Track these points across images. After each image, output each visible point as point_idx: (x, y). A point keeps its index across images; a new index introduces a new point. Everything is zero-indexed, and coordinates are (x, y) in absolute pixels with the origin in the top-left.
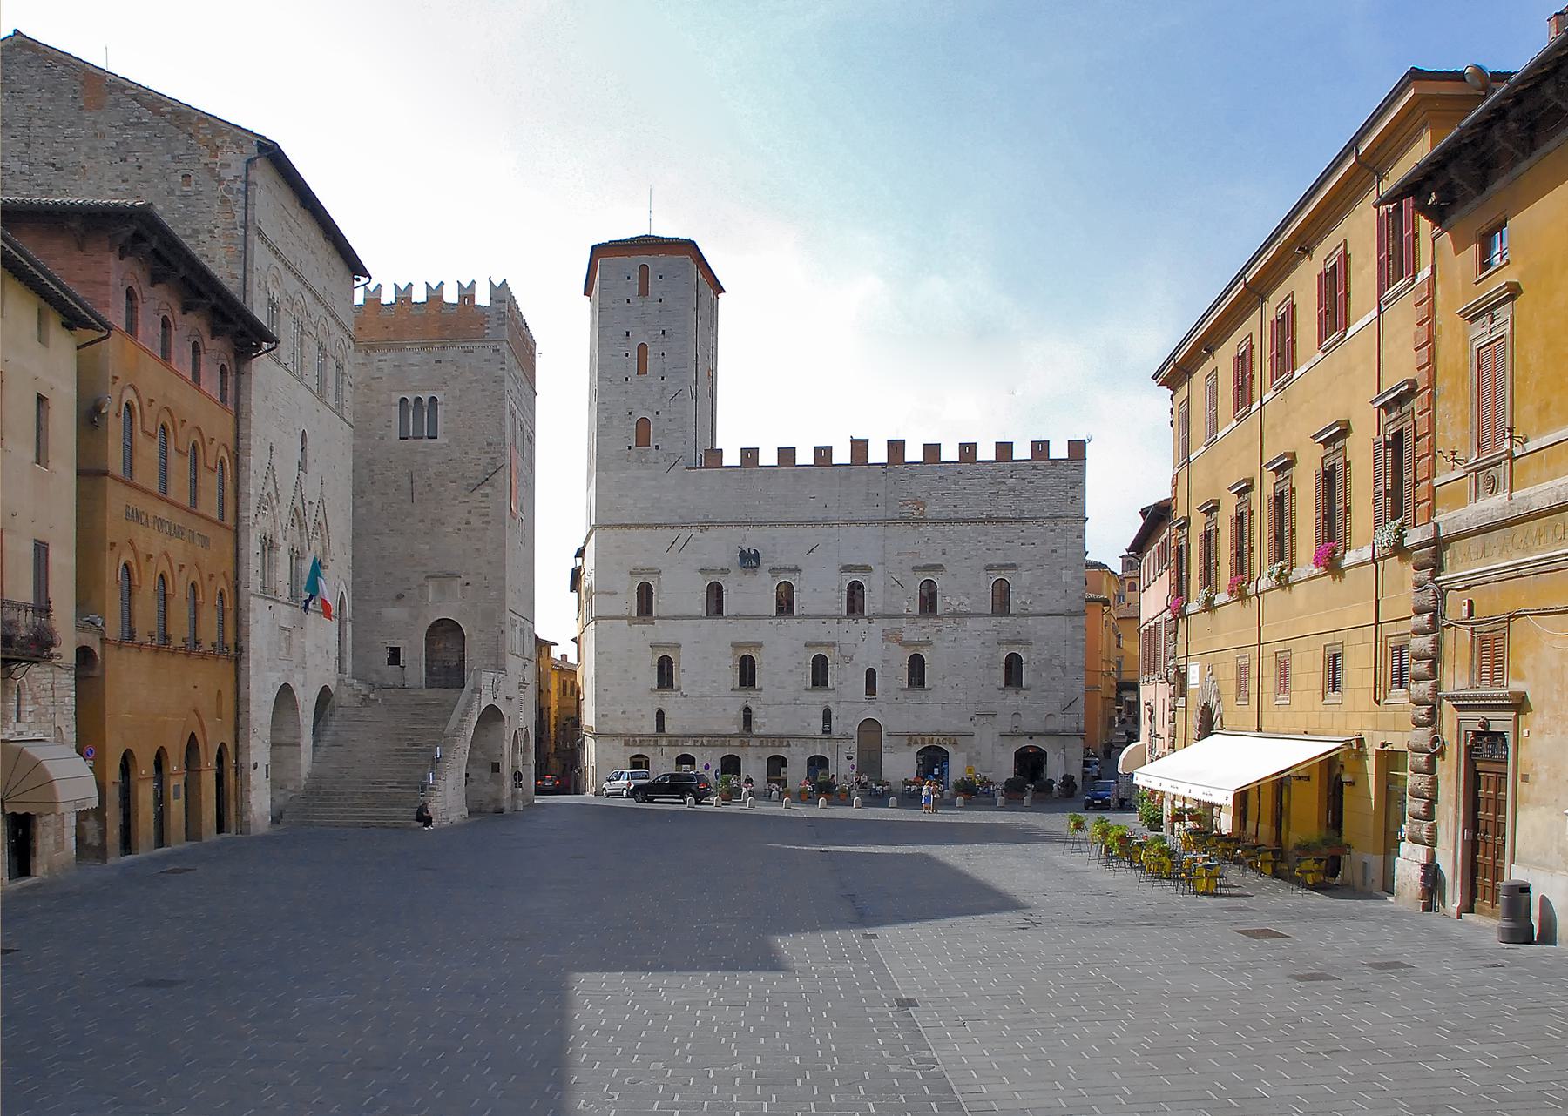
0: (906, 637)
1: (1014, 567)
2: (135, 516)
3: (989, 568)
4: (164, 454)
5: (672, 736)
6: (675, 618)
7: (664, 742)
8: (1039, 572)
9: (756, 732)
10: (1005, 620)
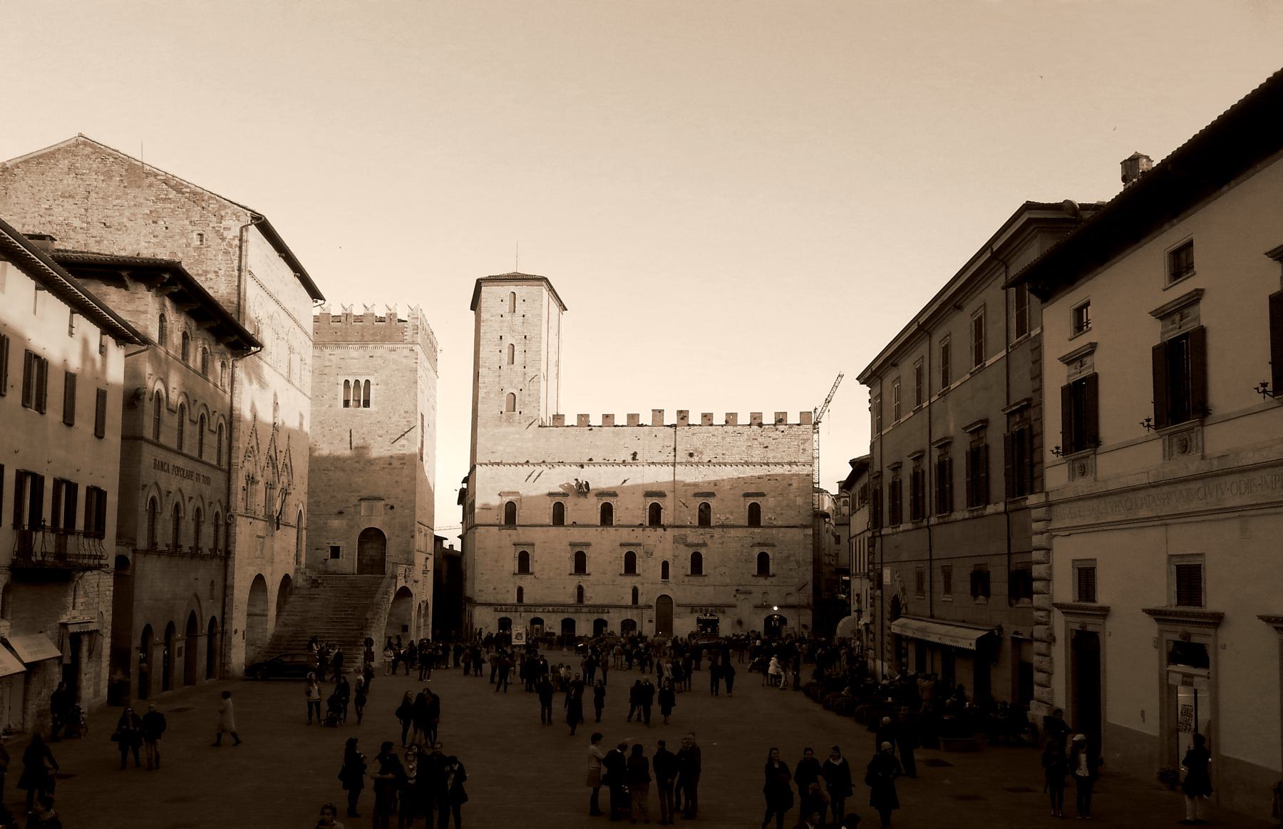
0: (689, 540)
1: (762, 495)
2: (160, 466)
3: (747, 495)
4: (181, 424)
6: (531, 526)
8: (780, 498)
9: (586, 602)
10: (757, 530)
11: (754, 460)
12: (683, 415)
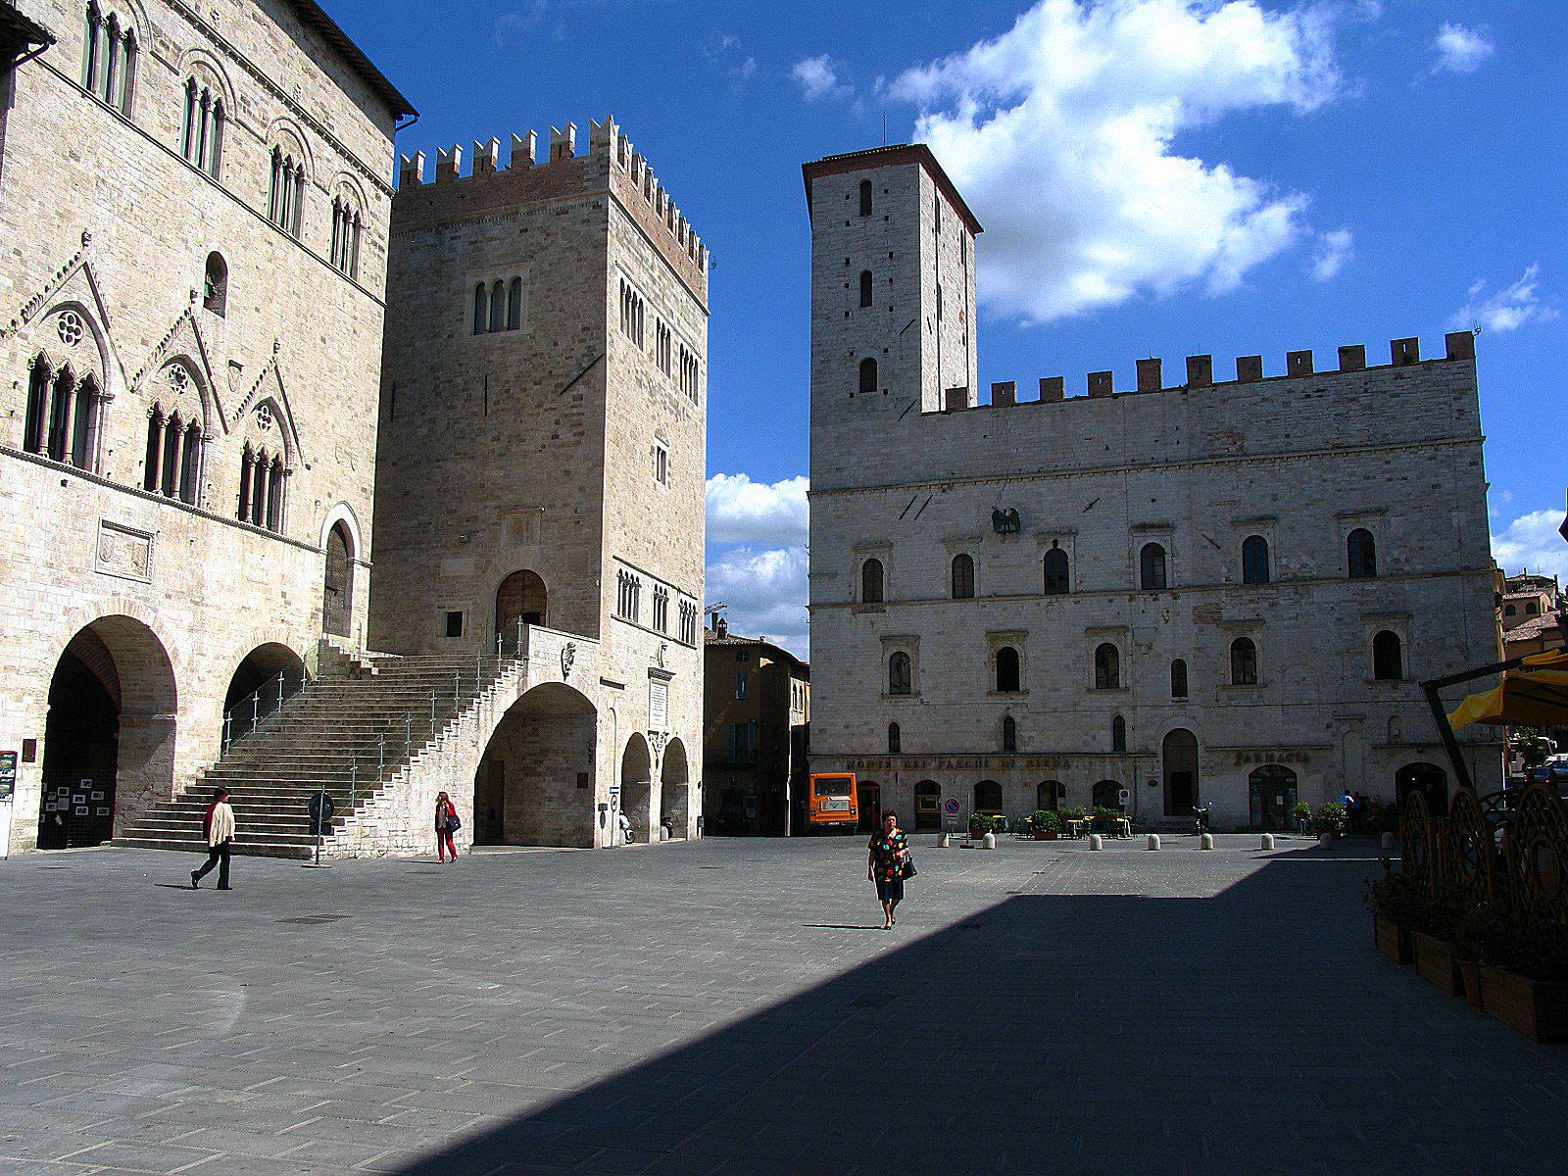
0: (1225, 615)
3: (1340, 516)
5: (913, 755)
7: (899, 763)
9: (1021, 748)
10: (1369, 586)
11: (1353, 442)
12: (1199, 366)
